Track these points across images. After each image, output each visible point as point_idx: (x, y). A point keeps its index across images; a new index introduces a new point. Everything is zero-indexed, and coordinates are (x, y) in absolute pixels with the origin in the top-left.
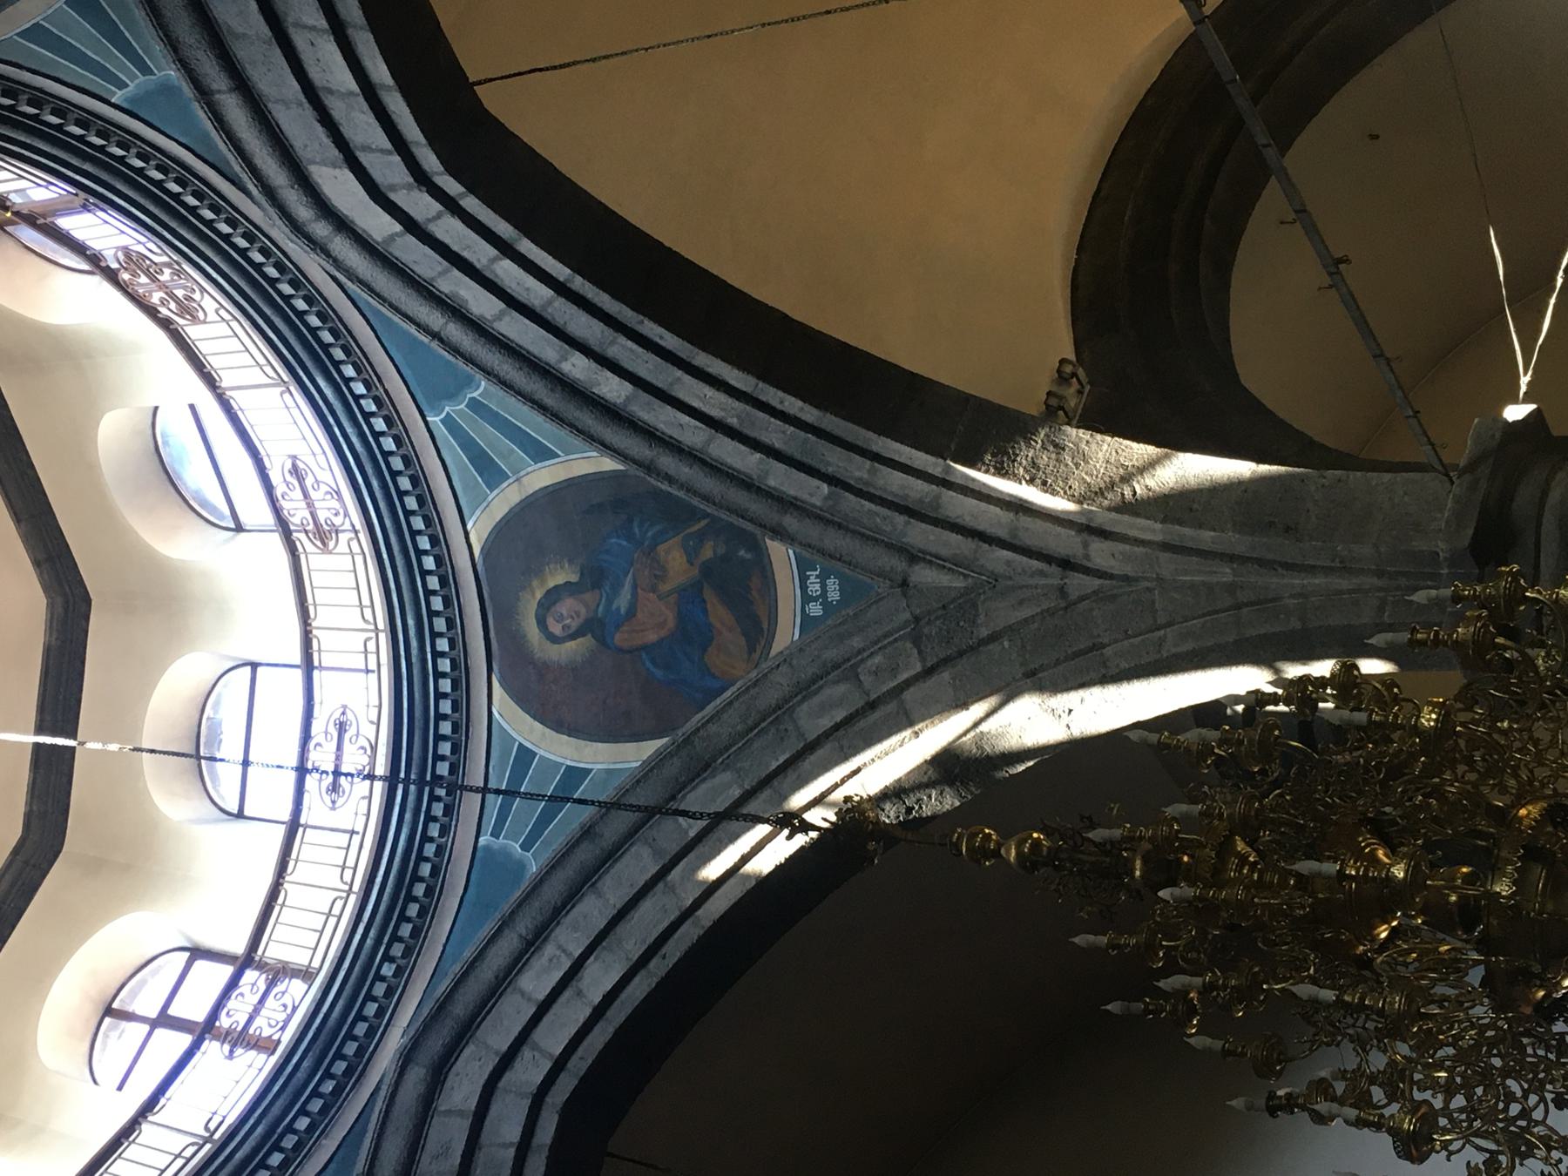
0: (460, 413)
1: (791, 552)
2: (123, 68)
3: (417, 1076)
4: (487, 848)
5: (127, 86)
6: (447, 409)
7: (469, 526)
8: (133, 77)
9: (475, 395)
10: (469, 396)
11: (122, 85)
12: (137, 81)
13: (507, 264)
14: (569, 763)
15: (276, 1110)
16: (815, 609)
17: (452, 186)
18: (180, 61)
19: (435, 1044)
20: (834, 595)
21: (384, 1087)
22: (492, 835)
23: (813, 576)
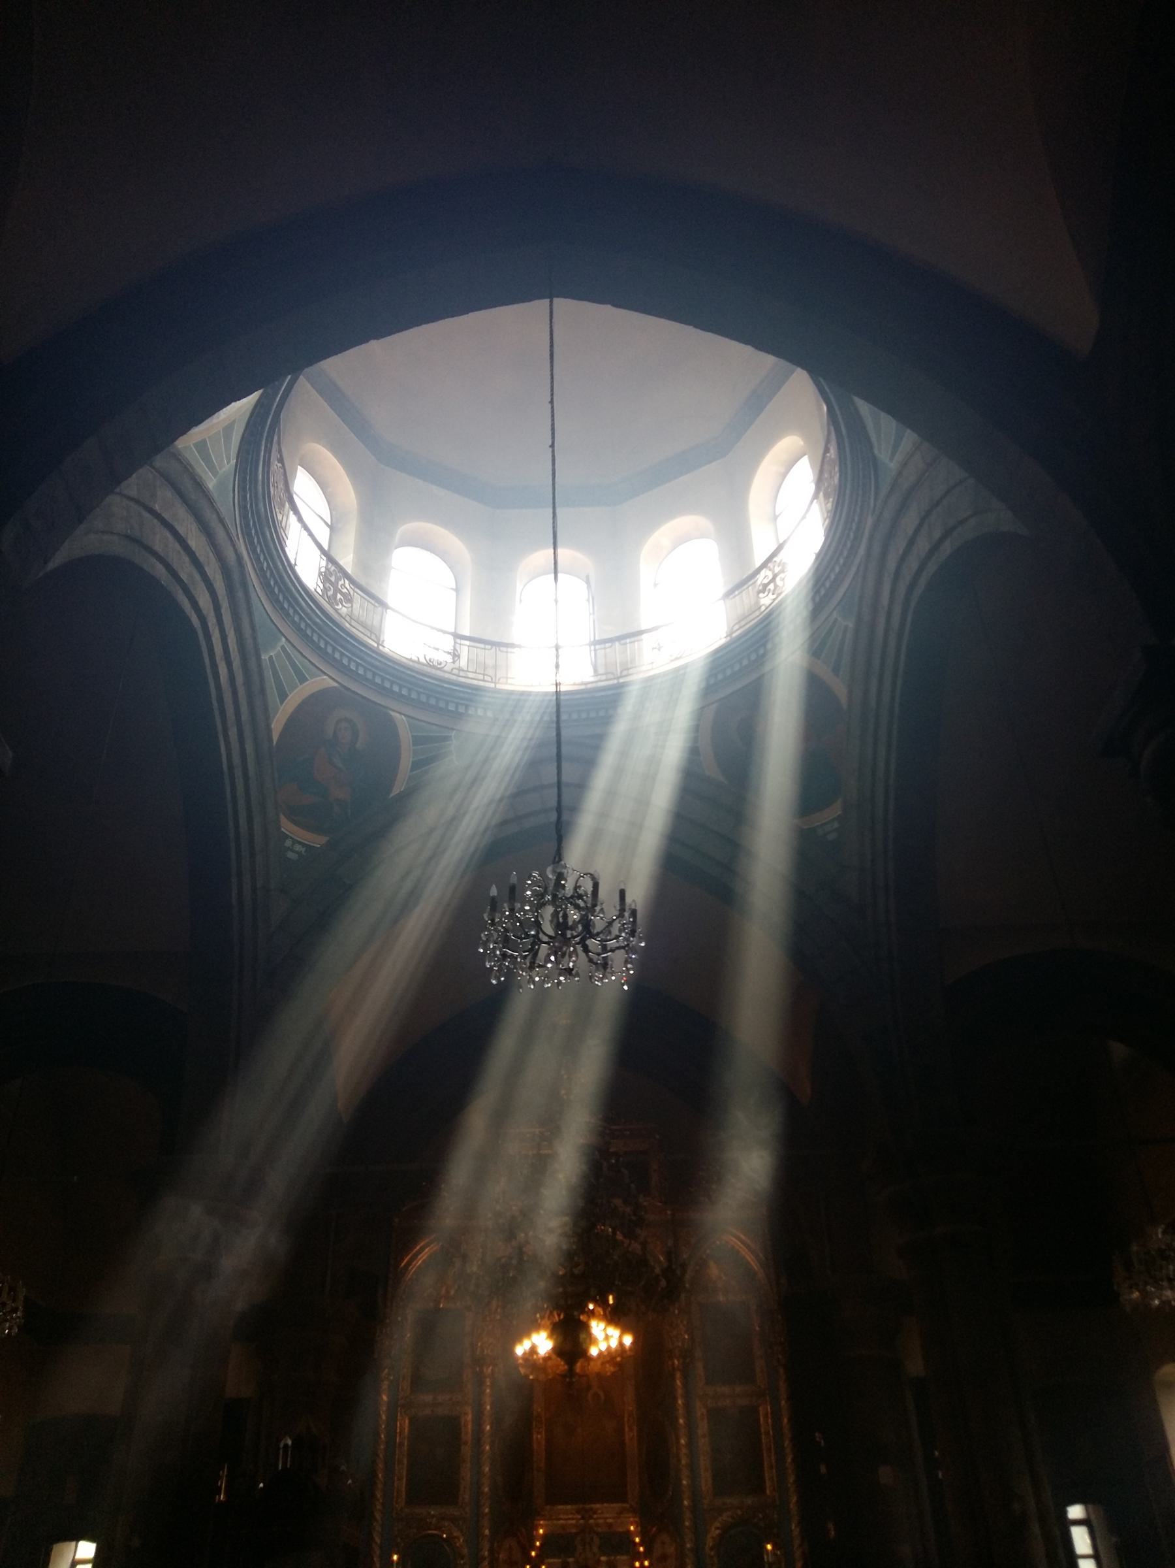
4: (280, 640)
7: (403, 717)
14: (289, 698)
15: (260, 488)
16: (288, 843)
19: (236, 576)
20: (290, 855)
21: (237, 541)
22: (283, 646)
23: (303, 850)
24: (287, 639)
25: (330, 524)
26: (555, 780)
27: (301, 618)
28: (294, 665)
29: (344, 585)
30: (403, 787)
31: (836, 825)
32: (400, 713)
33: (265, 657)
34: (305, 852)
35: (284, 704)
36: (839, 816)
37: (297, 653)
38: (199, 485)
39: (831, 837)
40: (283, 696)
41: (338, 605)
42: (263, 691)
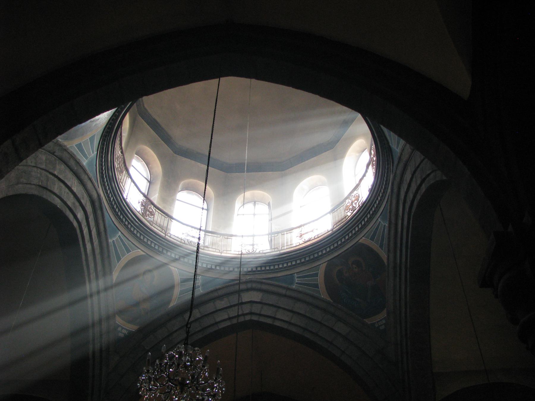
0: (199, 282)
1: (134, 330)
2: (301, 280)
3: (95, 195)
4: (118, 233)
5: (297, 278)
6: (201, 281)
7: (176, 269)
8: (298, 280)
9: (200, 288)
10: (201, 287)
11: (297, 278)
12: (296, 281)
13: (226, 317)
14: (122, 259)
15: (109, 164)
17: (248, 318)
18: (296, 290)
19: (97, 204)
24: (121, 232)
25: (149, 180)
26: (243, 301)
27: (129, 223)
28: (124, 244)
29: (151, 208)
30: (175, 303)
31: (384, 322)
32: (175, 267)
33: (110, 241)
34: (127, 333)
35: (119, 262)
36: (386, 317)
37: (126, 239)
38: (78, 163)
39: (382, 327)
40: (119, 259)
41: (147, 217)
42: (109, 256)
